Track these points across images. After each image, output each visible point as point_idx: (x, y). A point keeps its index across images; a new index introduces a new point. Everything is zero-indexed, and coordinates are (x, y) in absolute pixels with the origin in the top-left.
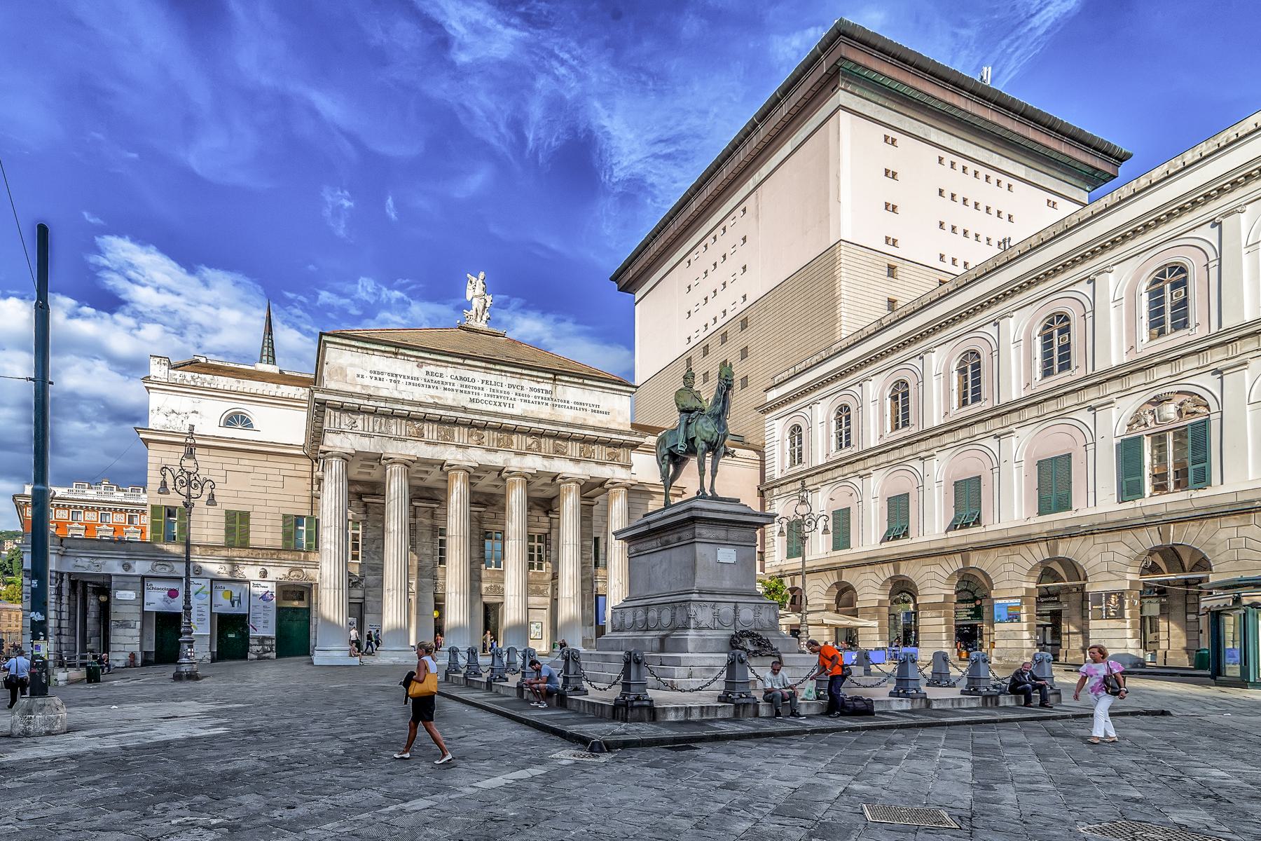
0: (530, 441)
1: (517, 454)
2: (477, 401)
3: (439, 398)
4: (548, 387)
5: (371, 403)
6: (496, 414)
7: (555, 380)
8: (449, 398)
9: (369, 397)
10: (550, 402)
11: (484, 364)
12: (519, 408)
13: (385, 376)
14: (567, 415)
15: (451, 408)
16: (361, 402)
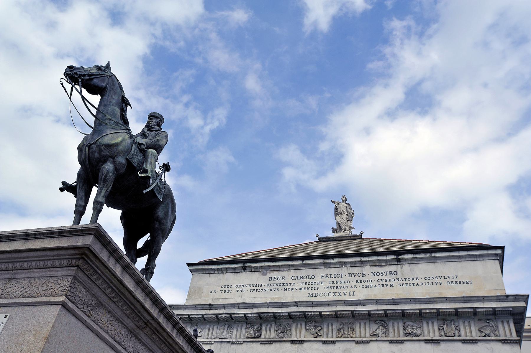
0: (374, 327)
1: (358, 342)
2: (316, 295)
3: (278, 298)
4: (392, 268)
5: (212, 312)
6: (328, 303)
7: (399, 260)
8: (289, 297)
9: (210, 307)
10: (396, 283)
11: (321, 261)
12: (361, 294)
13: (234, 289)
14: (418, 292)
15: (282, 304)
16: (203, 312)
